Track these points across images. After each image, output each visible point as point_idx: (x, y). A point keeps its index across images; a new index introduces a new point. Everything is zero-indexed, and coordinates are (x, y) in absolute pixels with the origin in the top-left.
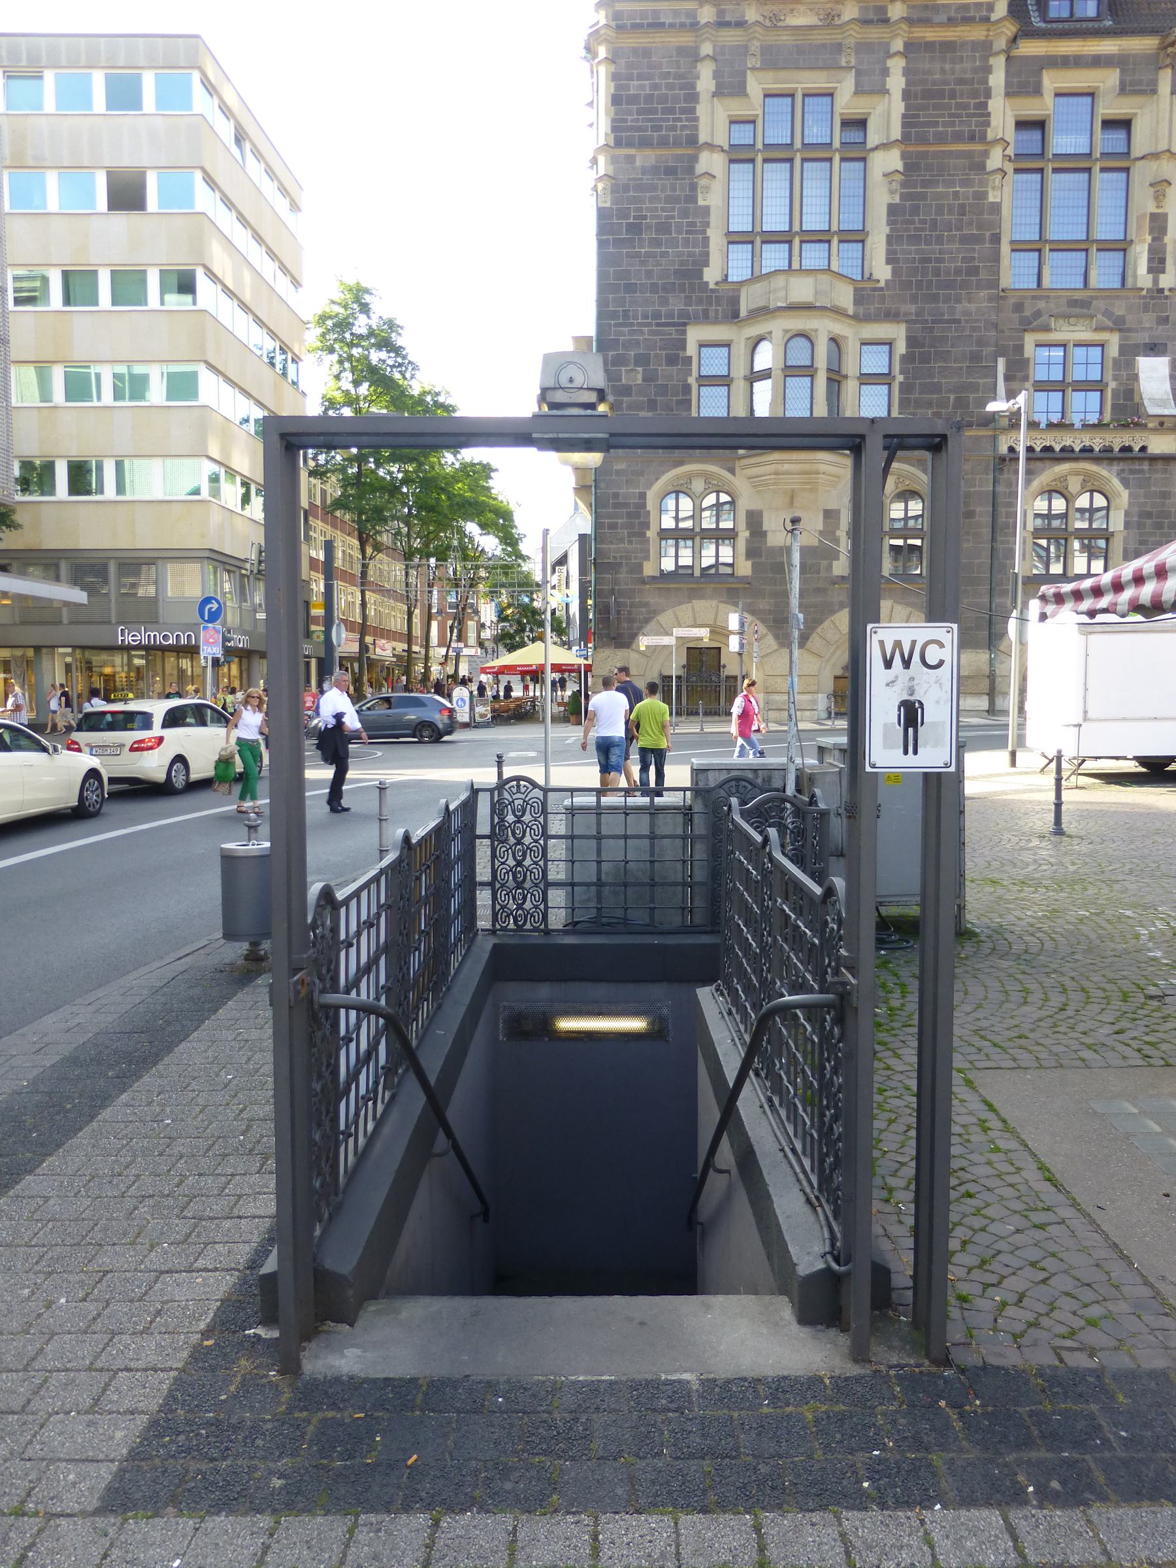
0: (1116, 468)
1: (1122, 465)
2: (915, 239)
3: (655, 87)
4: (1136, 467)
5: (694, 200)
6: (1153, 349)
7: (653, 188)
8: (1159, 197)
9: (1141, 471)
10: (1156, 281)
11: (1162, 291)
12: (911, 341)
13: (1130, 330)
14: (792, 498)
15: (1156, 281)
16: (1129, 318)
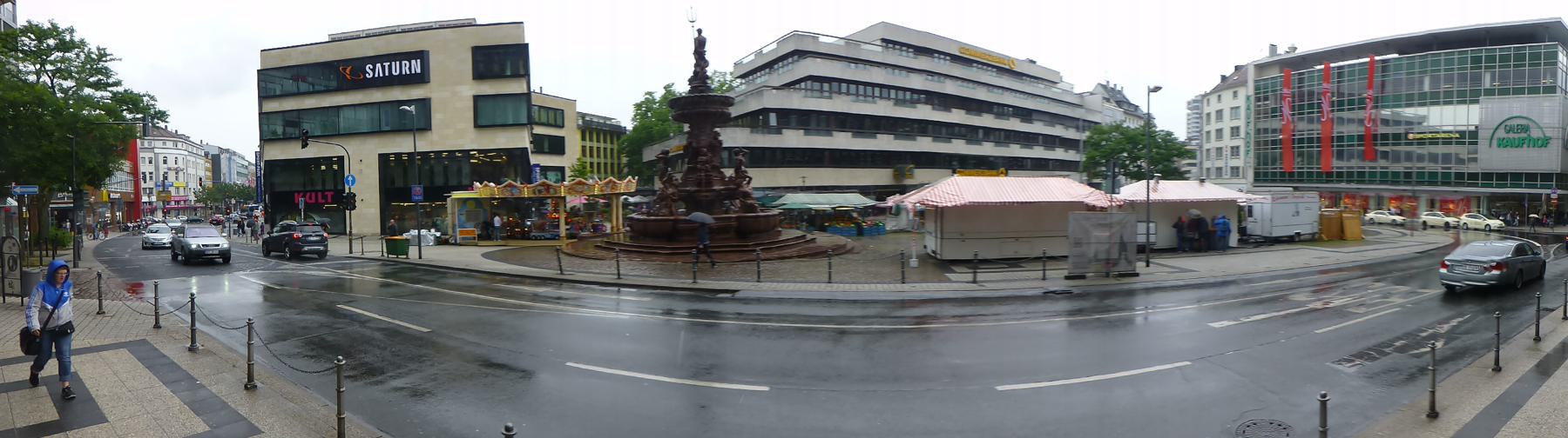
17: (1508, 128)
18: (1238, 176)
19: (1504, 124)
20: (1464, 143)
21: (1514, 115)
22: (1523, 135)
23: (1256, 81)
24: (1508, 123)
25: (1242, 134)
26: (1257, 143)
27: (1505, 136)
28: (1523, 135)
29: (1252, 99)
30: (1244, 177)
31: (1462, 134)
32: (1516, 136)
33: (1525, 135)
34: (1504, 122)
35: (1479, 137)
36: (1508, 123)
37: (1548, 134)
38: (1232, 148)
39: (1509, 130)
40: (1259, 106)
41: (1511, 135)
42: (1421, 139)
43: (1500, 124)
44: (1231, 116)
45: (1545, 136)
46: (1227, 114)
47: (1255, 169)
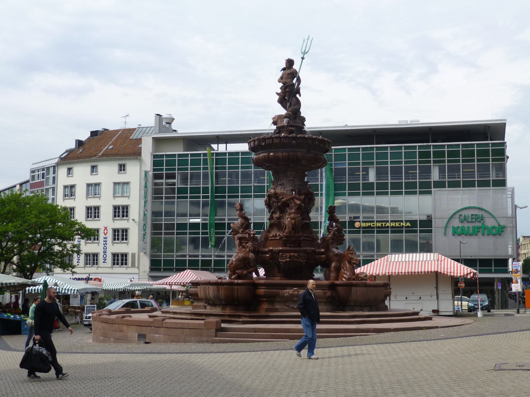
17: (462, 218)
18: (126, 264)
19: (460, 213)
20: (416, 232)
21: (484, 207)
22: (478, 224)
23: (155, 156)
24: (463, 213)
25: (135, 212)
26: (156, 227)
27: (460, 225)
28: (478, 224)
29: (151, 174)
30: (133, 265)
31: (413, 223)
32: (471, 225)
34: (459, 211)
35: (433, 227)
36: (463, 213)
37: (502, 223)
38: (115, 231)
40: (162, 184)
41: (466, 225)
42: (369, 227)
43: (455, 214)
44: (114, 193)
45: (499, 225)
46: (107, 190)
47: (152, 256)
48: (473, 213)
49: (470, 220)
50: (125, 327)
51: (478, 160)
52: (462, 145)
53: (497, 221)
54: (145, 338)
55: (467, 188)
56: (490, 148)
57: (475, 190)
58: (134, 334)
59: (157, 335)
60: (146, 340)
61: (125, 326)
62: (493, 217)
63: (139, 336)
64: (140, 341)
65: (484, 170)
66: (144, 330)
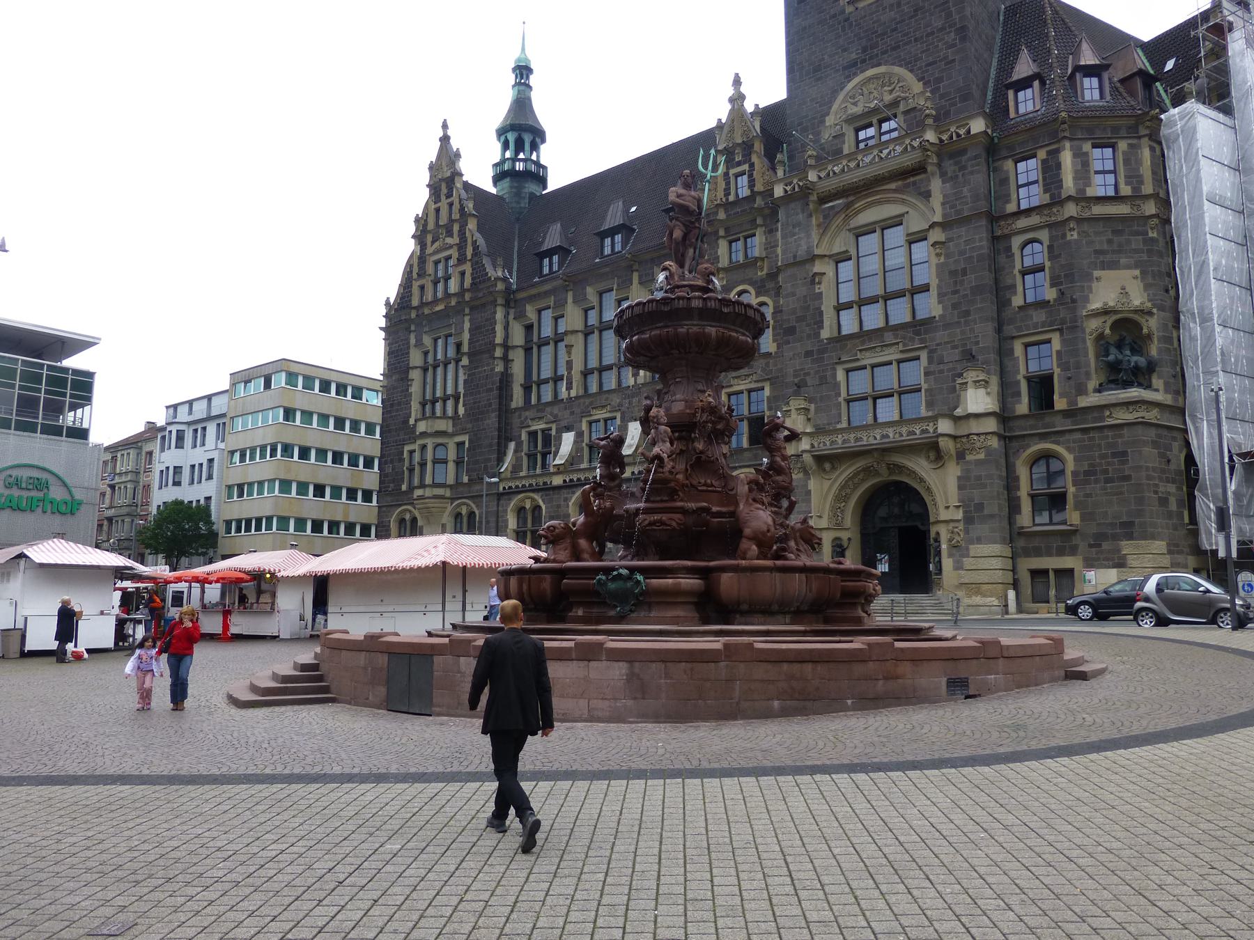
0: (540, 494)
1: (543, 493)
2: (472, 394)
3: (399, 346)
4: (548, 492)
5: (407, 390)
6: (568, 429)
7: (394, 388)
8: (569, 353)
9: (549, 495)
10: (569, 394)
11: (571, 398)
12: (470, 441)
13: (560, 420)
14: (428, 519)
15: (569, 394)
16: (560, 414)
19: (9, 472)
24: (15, 473)
27: (7, 492)
32: (25, 494)
33: (41, 495)
36: (15, 473)
37: (78, 495)
39: (17, 483)
41: (15, 492)
48: (32, 476)
49: (24, 485)
50: (905, 668)
51: (47, 392)
52: (22, 360)
53: (70, 492)
54: (967, 686)
55: (26, 434)
56: (70, 377)
57: (10, 434)
58: (936, 679)
59: (993, 676)
60: (968, 690)
61: (908, 663)
62: (65, 485)
63: (951, 682)
64: (954, 694)
65: (55, 409)
66: (962, 670)
